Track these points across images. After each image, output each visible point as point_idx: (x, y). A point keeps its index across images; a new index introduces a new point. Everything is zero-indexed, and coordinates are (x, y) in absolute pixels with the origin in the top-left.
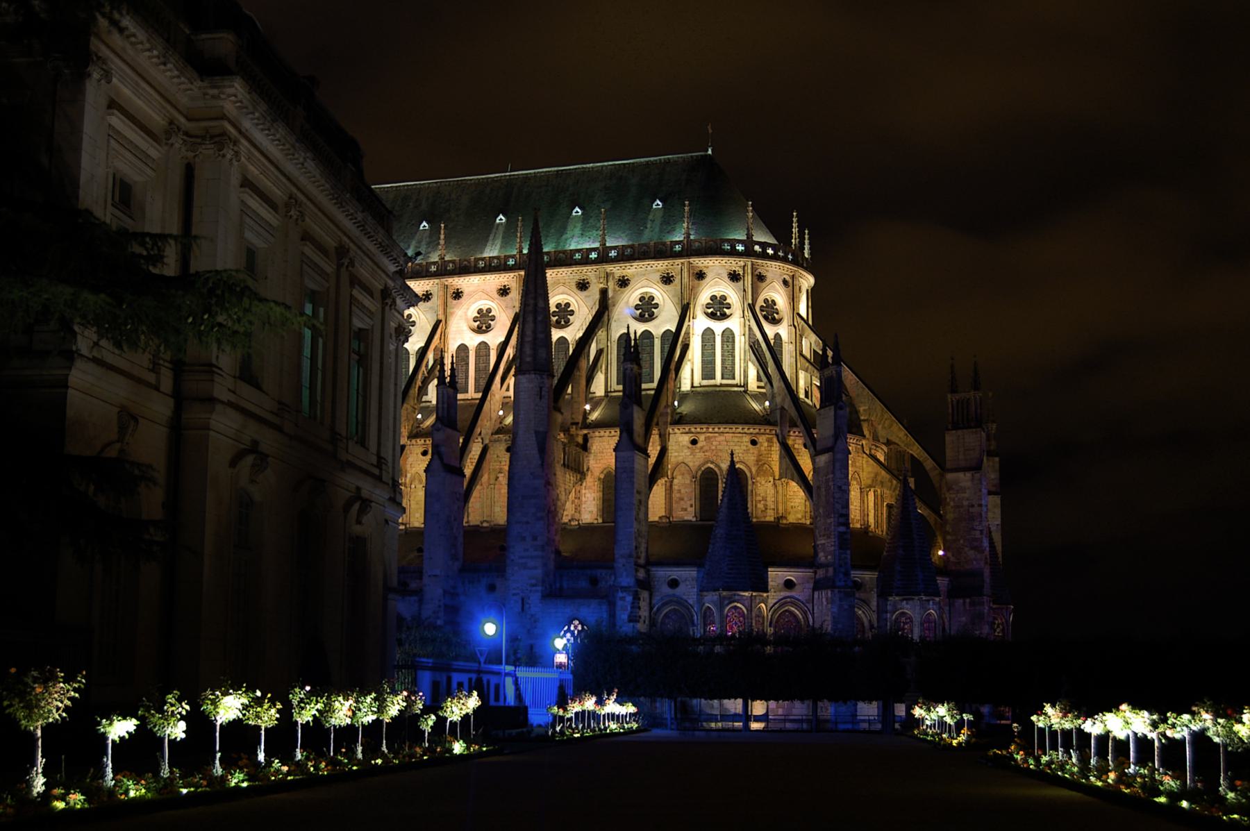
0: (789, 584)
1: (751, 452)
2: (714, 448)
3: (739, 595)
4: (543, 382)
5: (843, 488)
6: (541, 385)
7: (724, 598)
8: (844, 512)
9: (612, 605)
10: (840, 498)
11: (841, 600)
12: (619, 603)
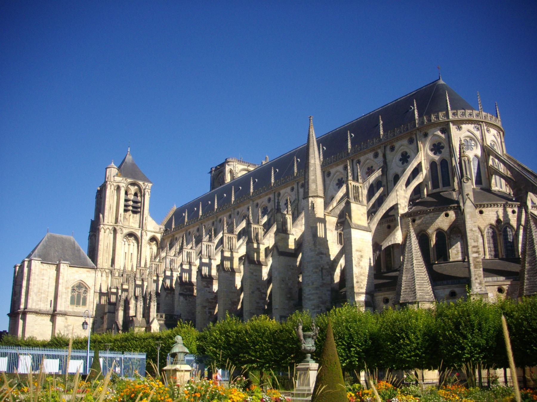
1: (445, 221)
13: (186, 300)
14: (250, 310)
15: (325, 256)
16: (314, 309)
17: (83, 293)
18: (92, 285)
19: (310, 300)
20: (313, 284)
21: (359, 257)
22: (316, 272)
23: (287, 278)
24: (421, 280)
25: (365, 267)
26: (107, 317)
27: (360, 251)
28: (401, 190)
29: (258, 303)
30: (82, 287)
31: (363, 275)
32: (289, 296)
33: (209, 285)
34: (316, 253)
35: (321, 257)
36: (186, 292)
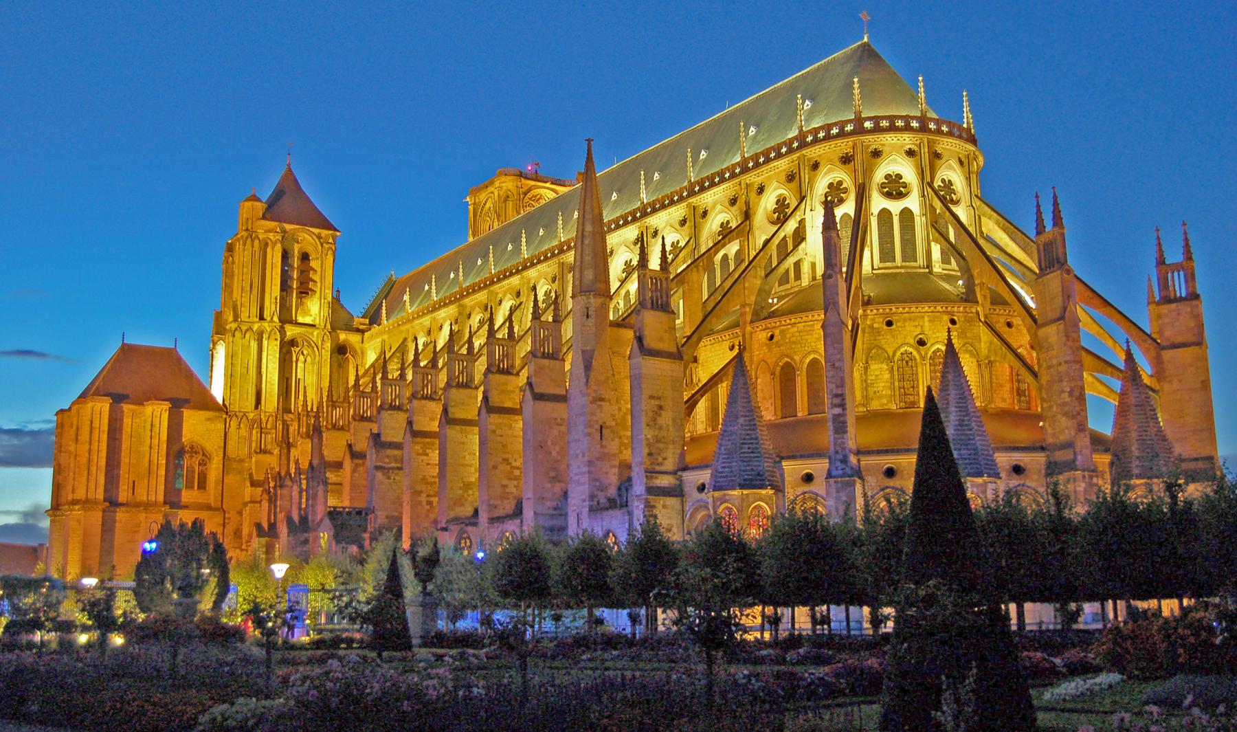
0: (808, 478)
4: (589, 303)
7: (718, 499)
9: (630, 514)
11: (838, 492)
13: (389, 478)
17: (200, 464)
19: (579, 483)
20: (583, 456)
21: (655, 409)
22: (589, 434)
23: (549, 443)
24: (748, 453)
26: (248, 512)
27: (659, 398)
28: (755, 277)
29: (505, 486)
31: (663, 440)
32: (552, 474)
34: (590, 398)
35: (600, 406)
36: (388, 463)
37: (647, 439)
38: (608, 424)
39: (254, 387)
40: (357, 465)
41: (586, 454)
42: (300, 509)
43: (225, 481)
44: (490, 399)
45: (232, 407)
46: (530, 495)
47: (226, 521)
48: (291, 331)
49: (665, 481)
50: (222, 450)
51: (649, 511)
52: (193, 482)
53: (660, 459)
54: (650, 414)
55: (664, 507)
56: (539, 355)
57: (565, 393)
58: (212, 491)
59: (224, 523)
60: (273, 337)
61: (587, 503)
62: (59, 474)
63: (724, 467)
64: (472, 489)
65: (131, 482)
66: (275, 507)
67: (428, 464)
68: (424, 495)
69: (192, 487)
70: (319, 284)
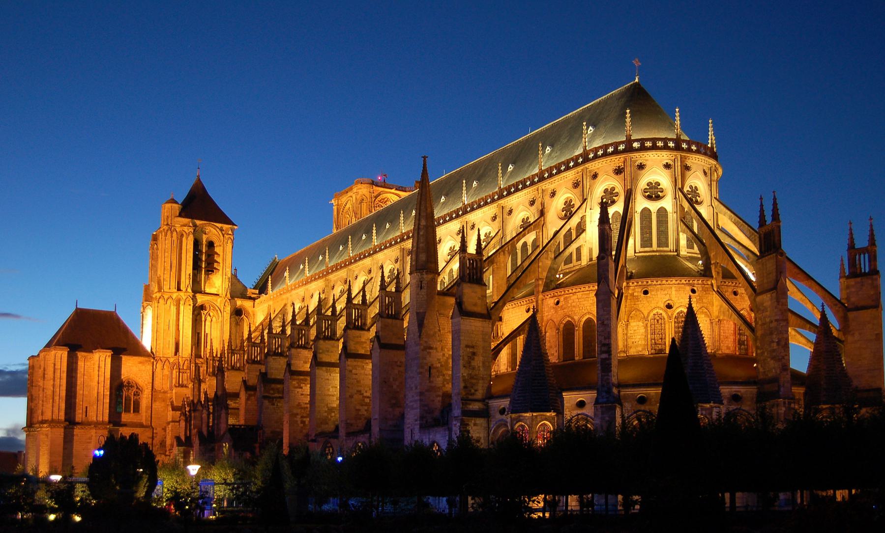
0: (581, 404)
2: (569, 305)
3: (522, 416)
4: (423, 278)
5: (605, 323)
6: (422, 280)
8: (607, 342)
9: (450, 430)
10: (603, 331)
11: (603, 413)
12: (454, 428)
13: (273, 404)
14: (346, 421)
15: (435, 351)
16: (416, 420)
17: (134, 395)
18: (148, 383)
20: (416, 388)
21: (470, 355)
22: (421, 373)
25: (479, 367)
26: (170, 428)
29: (359, 410)
30: (132, 387)
31: (475, 377)
32: (393, 401)
33: (302, 385)
34: (422, 347)
35: (429, 353)
36: (272, 394)
37: (464, 376)
38: (435, 366)
39: (174, 340)
40: (250, 395)
41: (418, 387)
42: (208, 426)
43: (153, 406)
44: (348, 348)
45: (157, 354)
46: (377, 416)
47: (154, 435)
48: (201, 299)
49: (476, 406)
50: (151, 385)
51: (463, 428)
52: (130, 407)
53: (473, 391)
54: (466, 358)
55: (475, 425)
56: (385, 316)
57: (403, 343)
58: (144, 414)
59: (153, 436)
60: (187, 303)
61: (419, 422)
62: (32, 402)
63: (518, 397)
64: (334, 412)
65: (84, 407)
66: (190, 426)
67: (302, 395)
68: (299, 417)
69: (129, 411)
70: (221, 264)
